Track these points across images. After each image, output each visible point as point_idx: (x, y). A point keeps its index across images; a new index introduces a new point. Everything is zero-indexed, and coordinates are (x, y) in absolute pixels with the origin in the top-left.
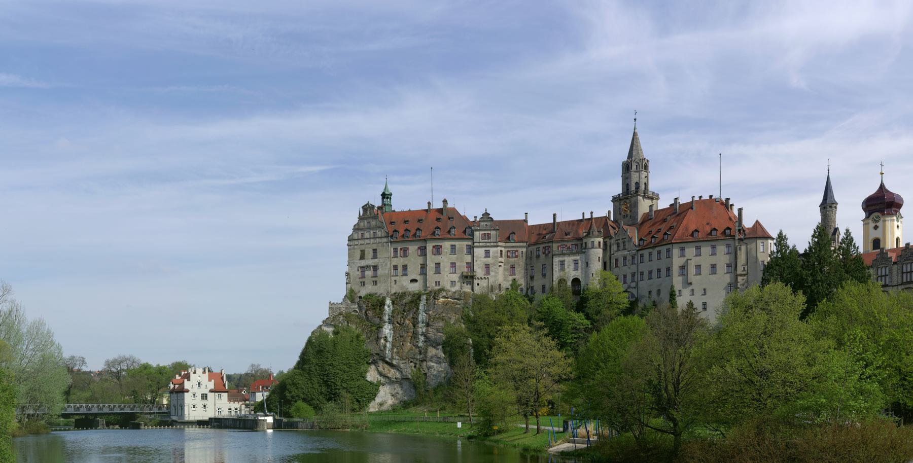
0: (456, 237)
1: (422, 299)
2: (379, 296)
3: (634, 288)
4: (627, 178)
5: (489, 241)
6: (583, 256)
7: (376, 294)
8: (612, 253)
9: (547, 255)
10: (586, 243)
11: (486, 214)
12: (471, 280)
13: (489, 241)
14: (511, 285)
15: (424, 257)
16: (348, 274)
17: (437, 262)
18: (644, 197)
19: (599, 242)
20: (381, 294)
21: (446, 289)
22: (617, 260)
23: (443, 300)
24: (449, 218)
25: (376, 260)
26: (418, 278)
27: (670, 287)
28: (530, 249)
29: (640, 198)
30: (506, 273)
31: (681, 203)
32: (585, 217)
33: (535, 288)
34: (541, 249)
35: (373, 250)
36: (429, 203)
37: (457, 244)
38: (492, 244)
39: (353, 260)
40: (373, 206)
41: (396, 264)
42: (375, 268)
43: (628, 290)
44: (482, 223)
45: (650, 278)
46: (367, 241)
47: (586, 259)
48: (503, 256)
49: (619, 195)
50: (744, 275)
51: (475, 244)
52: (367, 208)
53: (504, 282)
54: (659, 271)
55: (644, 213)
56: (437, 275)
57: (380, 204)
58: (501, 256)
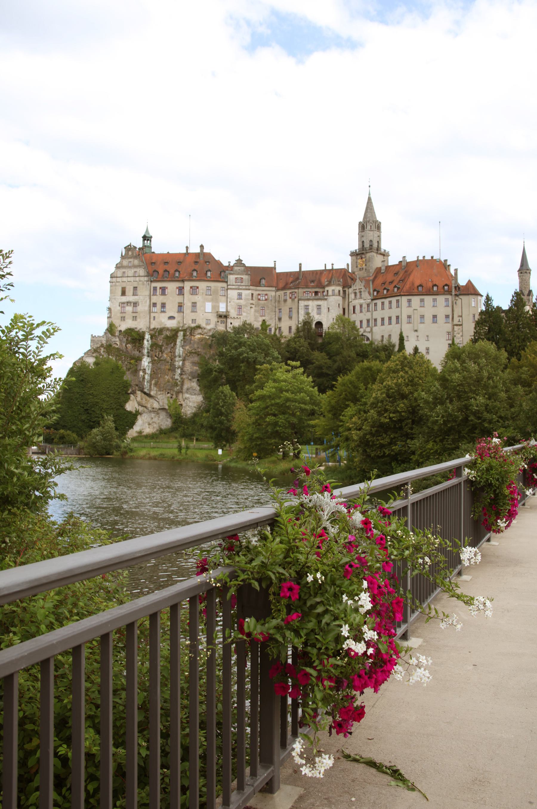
0: (212, 279)
1: (179, 335)
2: (139, 331)
3: (369, 332)
4: (363, 236)
5: (242, 284)
6: (325, 302)
7: (136, 328)
8: (350, 301)
9: (293, 300)
10: (328, 291)
11: (239, 262)
12: (225, 320)
13: (242, 284)
14: (261, 325)
15: (182, 296)
16: (109, 309)
17: (194, 301)
18: (377, 253)
19: (339, 291)
20: (141, 329)
21: (201, 326)
22: (354, 307)
23: (199, 336)
24: (206, 262)
25: (136, 297)
26: (176, 315)
27: (399, 333)
28: (278, 293)
29: (375, 254)
30: (257, 314)
31: (408, 261)
32: (327, 268)
33: (282, 329)
34: (288, 294)
35: (134, 288)
36: (187, 248)
37: (213, 285)
38: (244, 287)
39: (114, 296)
40: (135, 248)
41: (155, 302)
42: (135, 304)
43: (364, 334)
44: (236, 268)
45: (383, 324)
46: (129, 279)
47: (327, 305)
48: (254, 298)
49: (356, 250)
50: (460, 325)
51: (229, 287)
52: (129, 248)
53: (255, 322)
54: (390, 318)
55: (377, 268)
56: (193, 314)
57: (141, 246)
58: (252, 299)
